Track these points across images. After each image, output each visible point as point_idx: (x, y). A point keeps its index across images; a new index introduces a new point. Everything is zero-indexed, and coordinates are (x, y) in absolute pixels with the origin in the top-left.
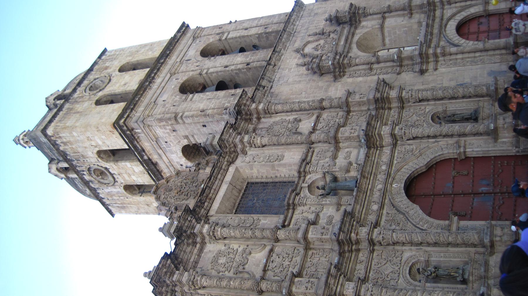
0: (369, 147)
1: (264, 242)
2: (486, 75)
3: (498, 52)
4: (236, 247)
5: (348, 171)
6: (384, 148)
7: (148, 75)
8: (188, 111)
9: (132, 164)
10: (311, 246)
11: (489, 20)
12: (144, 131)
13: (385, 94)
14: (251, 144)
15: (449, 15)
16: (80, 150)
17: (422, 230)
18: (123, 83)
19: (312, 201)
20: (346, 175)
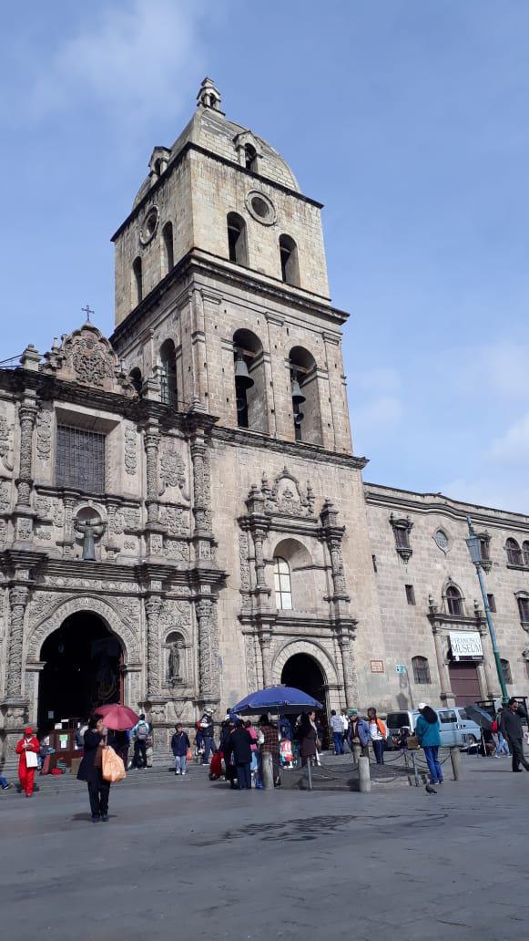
1: (17, 470)
2: (232, 689)
4: (11, 437)
10: (10, 522)
18: (261, 246)
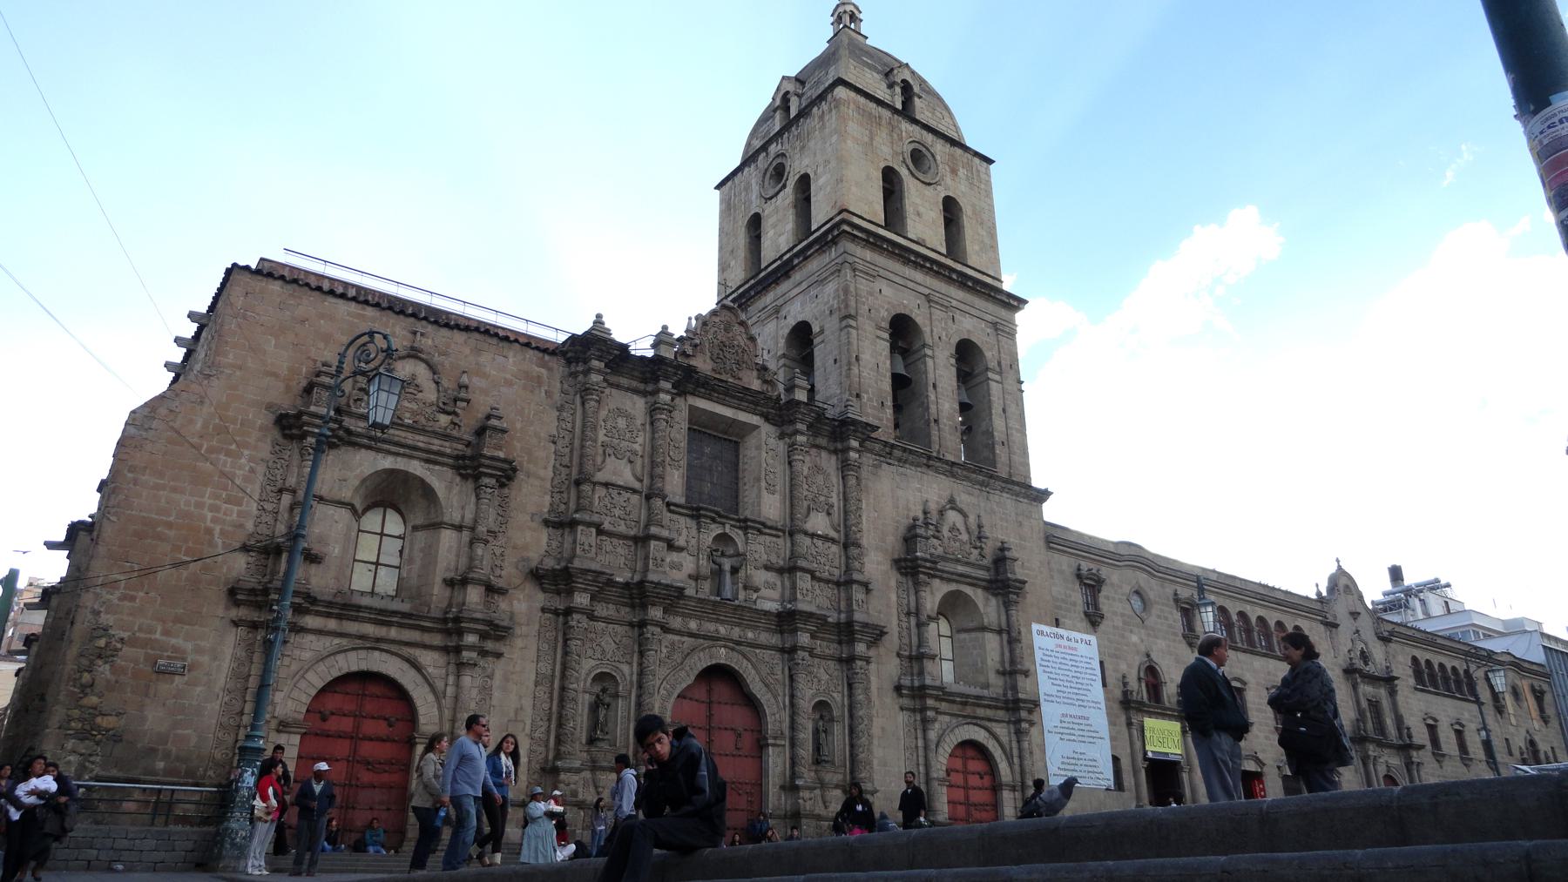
0: (779, 615)
1: (646, 481)
4: (640, 440)
6: (779, 635)
8: (858, 335)
9: (791, 233)
10: (640, 545)
14: (792, 448)
16: (812, 144)
18: (922, 210)
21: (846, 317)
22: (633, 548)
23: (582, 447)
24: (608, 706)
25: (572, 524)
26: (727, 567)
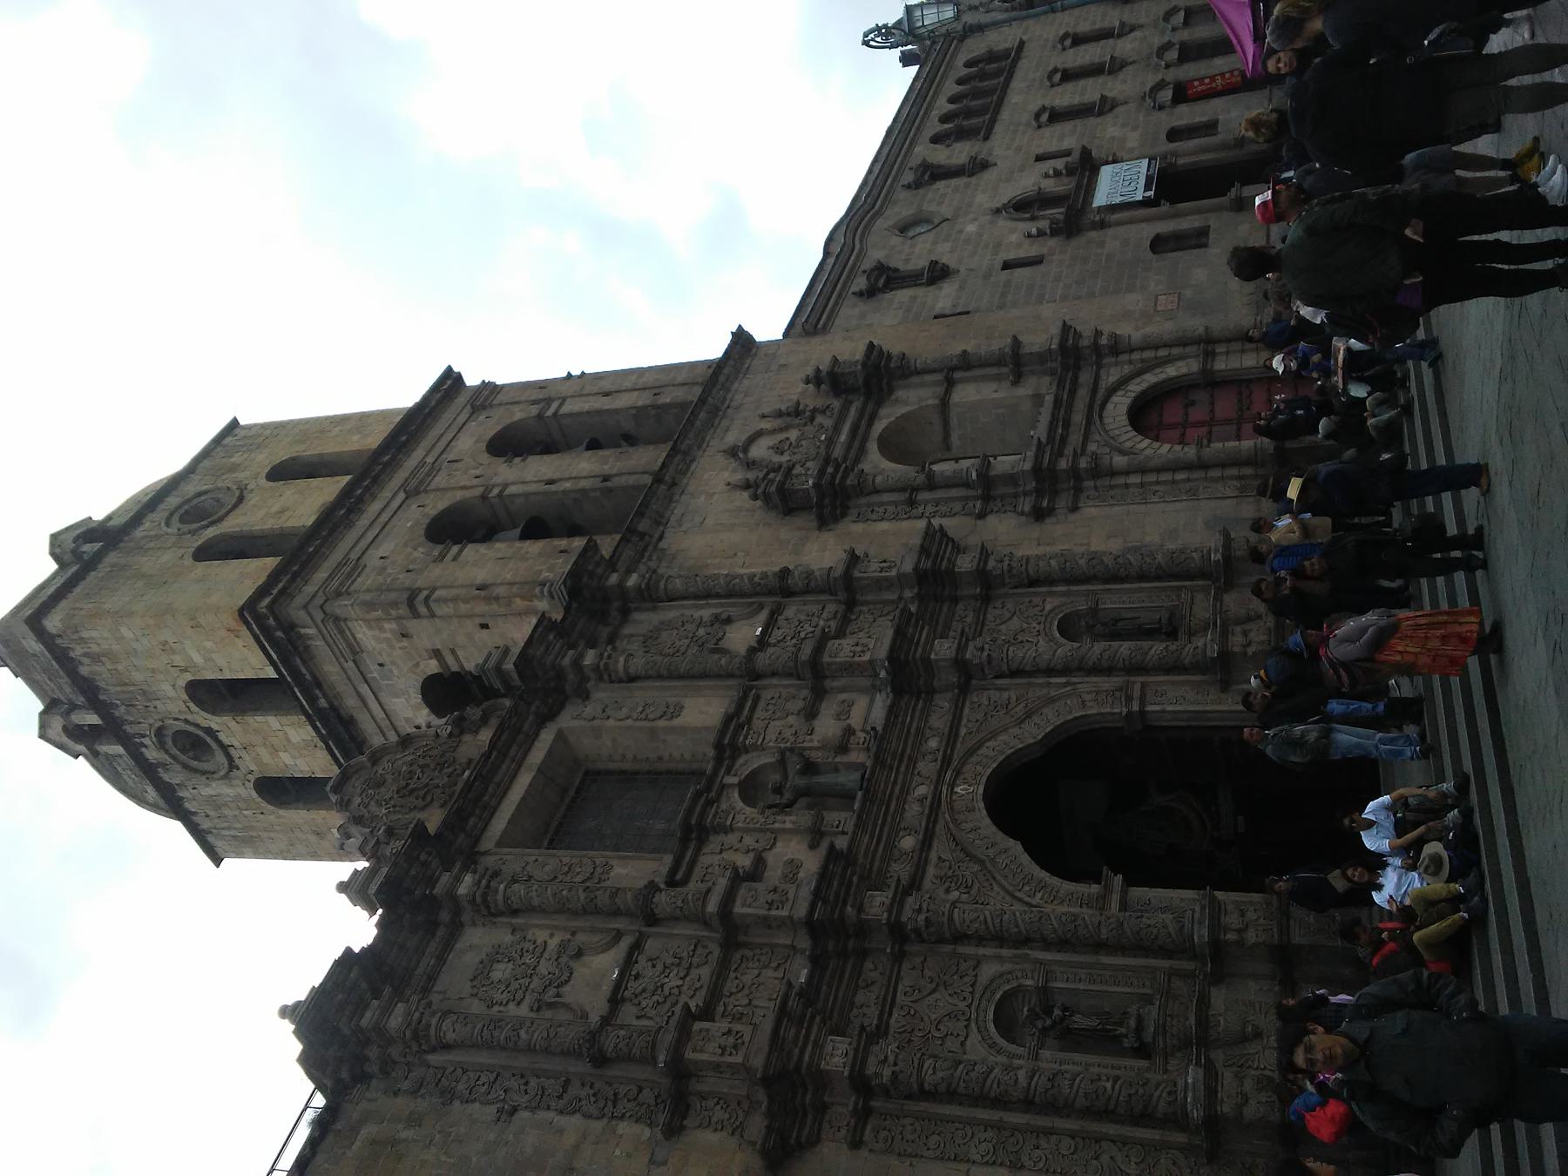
3: (1233, 471)
4: (541, 936)
5: (843, 748)
6: (937, 696)
7: (346, 493)
8: (443, 587)
9: (284, 720)
10: (742, 938)
11: (1212, 396)
12: (325, 632)
13: (945, 563)
14: (604, 674)
15: (1112, 379)
16: (138, 677)
17: (1030, 905)
19: (748, 820)
20: (838, 759)
21: (411, 602)
22: (749, 953)
23: (530, 1049)
24: (1065, 1009)
25: (680, 1072)
26: (801, 782)
